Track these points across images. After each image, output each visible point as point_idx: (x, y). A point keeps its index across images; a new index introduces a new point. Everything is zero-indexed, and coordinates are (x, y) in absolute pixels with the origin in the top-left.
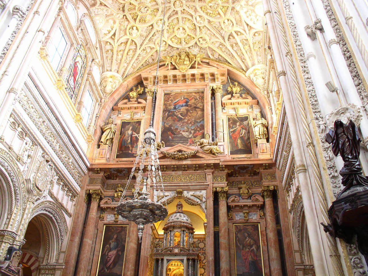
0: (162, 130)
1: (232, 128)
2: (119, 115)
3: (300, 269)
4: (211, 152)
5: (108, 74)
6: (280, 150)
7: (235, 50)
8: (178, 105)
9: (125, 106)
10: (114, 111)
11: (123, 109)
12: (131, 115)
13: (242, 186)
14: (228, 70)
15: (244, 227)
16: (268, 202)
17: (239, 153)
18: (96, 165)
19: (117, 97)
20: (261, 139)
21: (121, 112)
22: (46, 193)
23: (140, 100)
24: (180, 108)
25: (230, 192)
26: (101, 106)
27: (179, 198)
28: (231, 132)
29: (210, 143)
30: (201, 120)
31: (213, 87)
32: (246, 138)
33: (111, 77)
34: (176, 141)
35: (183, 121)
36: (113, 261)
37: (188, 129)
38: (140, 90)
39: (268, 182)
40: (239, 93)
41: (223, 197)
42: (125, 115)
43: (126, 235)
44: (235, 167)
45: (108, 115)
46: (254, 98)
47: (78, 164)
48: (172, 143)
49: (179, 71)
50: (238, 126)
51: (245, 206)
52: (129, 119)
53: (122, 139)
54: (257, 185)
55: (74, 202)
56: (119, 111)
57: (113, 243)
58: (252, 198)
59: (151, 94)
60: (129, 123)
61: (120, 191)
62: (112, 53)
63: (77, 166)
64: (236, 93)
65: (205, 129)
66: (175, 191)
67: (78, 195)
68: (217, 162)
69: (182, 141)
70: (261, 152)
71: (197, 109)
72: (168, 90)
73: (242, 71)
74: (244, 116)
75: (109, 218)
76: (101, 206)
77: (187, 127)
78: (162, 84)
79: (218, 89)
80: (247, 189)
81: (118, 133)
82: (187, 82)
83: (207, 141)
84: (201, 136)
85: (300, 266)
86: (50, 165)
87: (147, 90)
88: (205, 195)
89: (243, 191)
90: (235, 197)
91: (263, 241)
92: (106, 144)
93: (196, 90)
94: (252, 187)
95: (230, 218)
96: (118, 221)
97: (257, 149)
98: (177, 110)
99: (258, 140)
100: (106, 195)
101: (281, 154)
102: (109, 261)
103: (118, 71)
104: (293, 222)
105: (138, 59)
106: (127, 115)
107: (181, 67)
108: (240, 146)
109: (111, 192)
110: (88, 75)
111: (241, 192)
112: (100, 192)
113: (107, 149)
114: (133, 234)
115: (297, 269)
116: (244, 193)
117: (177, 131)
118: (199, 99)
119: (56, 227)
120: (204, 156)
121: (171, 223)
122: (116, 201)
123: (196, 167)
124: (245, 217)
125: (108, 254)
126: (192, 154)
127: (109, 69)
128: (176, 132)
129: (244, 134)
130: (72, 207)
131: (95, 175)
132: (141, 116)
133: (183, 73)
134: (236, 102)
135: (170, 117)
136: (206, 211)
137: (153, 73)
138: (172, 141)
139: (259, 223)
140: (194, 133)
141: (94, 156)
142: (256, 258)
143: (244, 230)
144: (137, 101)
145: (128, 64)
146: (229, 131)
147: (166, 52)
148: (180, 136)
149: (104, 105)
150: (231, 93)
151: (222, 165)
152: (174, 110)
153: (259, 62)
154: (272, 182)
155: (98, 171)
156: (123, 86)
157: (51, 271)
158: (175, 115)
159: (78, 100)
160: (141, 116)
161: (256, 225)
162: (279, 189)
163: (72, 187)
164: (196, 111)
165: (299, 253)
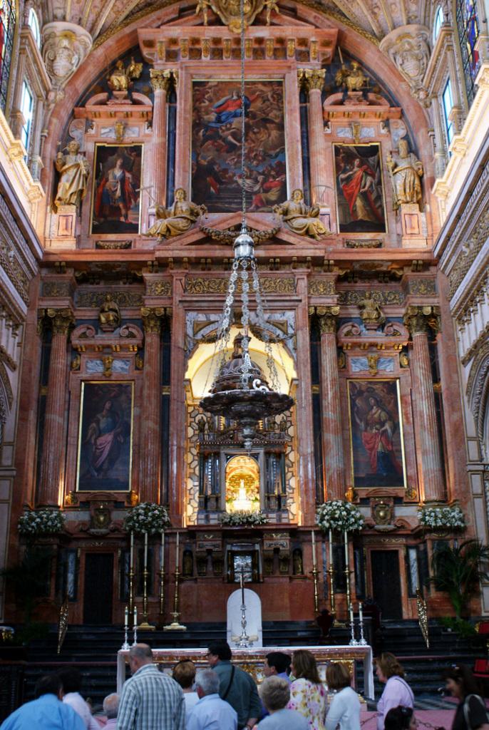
0: (194, 172)
1: (345, 171)
2: (90, 130)
3: (475, 472)
6: (454, 240)
8: (224, 113)
9: (103, 109)
10: (76, 121)
12: (117, 132)
13: (366, 302)
15: (369, 385)
16: (419, 336)
17: (358, 230)
19: (81, 85)
20: (407, 202)
21: (94, 123)
23: (136, 96)
24: (231, 120)
25: (344, 314)
26: (49, 110)
28: (342, 180)
29: (303, 212)
30: (278, 150)
32: (373, 196)
33: (66, 36)
34: (224, 198)
36: (108, 455)
37: (251, 171)
38: (136, 69)
39: (421, 297)
41: (329, 327)
42: (103, 131)
43: (131, 403)
44: (354, 264)
45: (64, 130)
47: (24, 258)
48: (216, 202)
49: (229, 29)
50: (359, 166)
52: (112, 140)
53: (100, 190)
54: (395, 301)
55: (17, 337)
56: (87, 119)
57: (105, 419)
58: (386, 328)
60: (113, 151)
63: (20, 260)
64: (354, 90)
67: (25, 323)
68: (319, 253)
70: (409, 232)
71: (268, 125)
74: (369, 145)
75: (92, 368)
77: (248, 168)
79: (315, 80)
80: (377, 309)
81: (93, 174)
83: (298, 206)
84: (279, 188)
85: (477, 466)
87: (152, 73)
88: (291, 322)
90: (353, 326)
91: (405, 414)
92: (69, 204)
94: (386, 304)
95: (343, 367)
97: (399, 224)
98: (224, 124)
99: (403, 206)
101: (456, 247)
102: (100, 456)
103: (80, 19)
104: (469, 385)
106: (107, 130)
108: (361, 215)
109: (89, 311)
110: (22, 38)
111: (365, 316)
112: (70, 314)
113: (75, 215)
114: (151, 404)
115: (470, 471)
116: (370, 319)
117: (227, 176)
118: (271, 100)
120: (291, 239)
121: (228, 379)
122: (105, 332)
123: (275, 263)
124: (371, 367)
125: (95, 442)
126: (267, 236)
127: (59, 13)
129: (369, 187)
130: (14, 350)
131: (54, 275)
132: (142, 134)
133: (237, 36)
134: (354, 112)
135: (210, 142)
136: (295, 355)
137: (167, 30)
138: (217, 198)
139: (399, 378)
140: (264, 181)
141: (47, 231)
142: (390, 447)
143: (368, 392)
144: (129, 97)
146: (337, 178)
148: (234, 188)
149: (55, 107)
153: (413, 18)
154: (428, 297)
155: (61, 267)
158: (220, 137)
159: (10, 106)
160: (142, 134)
161: (391, 383)
162: (442, 314)
163: (15, 309)
164: (267, 129)
165: (476, 442)
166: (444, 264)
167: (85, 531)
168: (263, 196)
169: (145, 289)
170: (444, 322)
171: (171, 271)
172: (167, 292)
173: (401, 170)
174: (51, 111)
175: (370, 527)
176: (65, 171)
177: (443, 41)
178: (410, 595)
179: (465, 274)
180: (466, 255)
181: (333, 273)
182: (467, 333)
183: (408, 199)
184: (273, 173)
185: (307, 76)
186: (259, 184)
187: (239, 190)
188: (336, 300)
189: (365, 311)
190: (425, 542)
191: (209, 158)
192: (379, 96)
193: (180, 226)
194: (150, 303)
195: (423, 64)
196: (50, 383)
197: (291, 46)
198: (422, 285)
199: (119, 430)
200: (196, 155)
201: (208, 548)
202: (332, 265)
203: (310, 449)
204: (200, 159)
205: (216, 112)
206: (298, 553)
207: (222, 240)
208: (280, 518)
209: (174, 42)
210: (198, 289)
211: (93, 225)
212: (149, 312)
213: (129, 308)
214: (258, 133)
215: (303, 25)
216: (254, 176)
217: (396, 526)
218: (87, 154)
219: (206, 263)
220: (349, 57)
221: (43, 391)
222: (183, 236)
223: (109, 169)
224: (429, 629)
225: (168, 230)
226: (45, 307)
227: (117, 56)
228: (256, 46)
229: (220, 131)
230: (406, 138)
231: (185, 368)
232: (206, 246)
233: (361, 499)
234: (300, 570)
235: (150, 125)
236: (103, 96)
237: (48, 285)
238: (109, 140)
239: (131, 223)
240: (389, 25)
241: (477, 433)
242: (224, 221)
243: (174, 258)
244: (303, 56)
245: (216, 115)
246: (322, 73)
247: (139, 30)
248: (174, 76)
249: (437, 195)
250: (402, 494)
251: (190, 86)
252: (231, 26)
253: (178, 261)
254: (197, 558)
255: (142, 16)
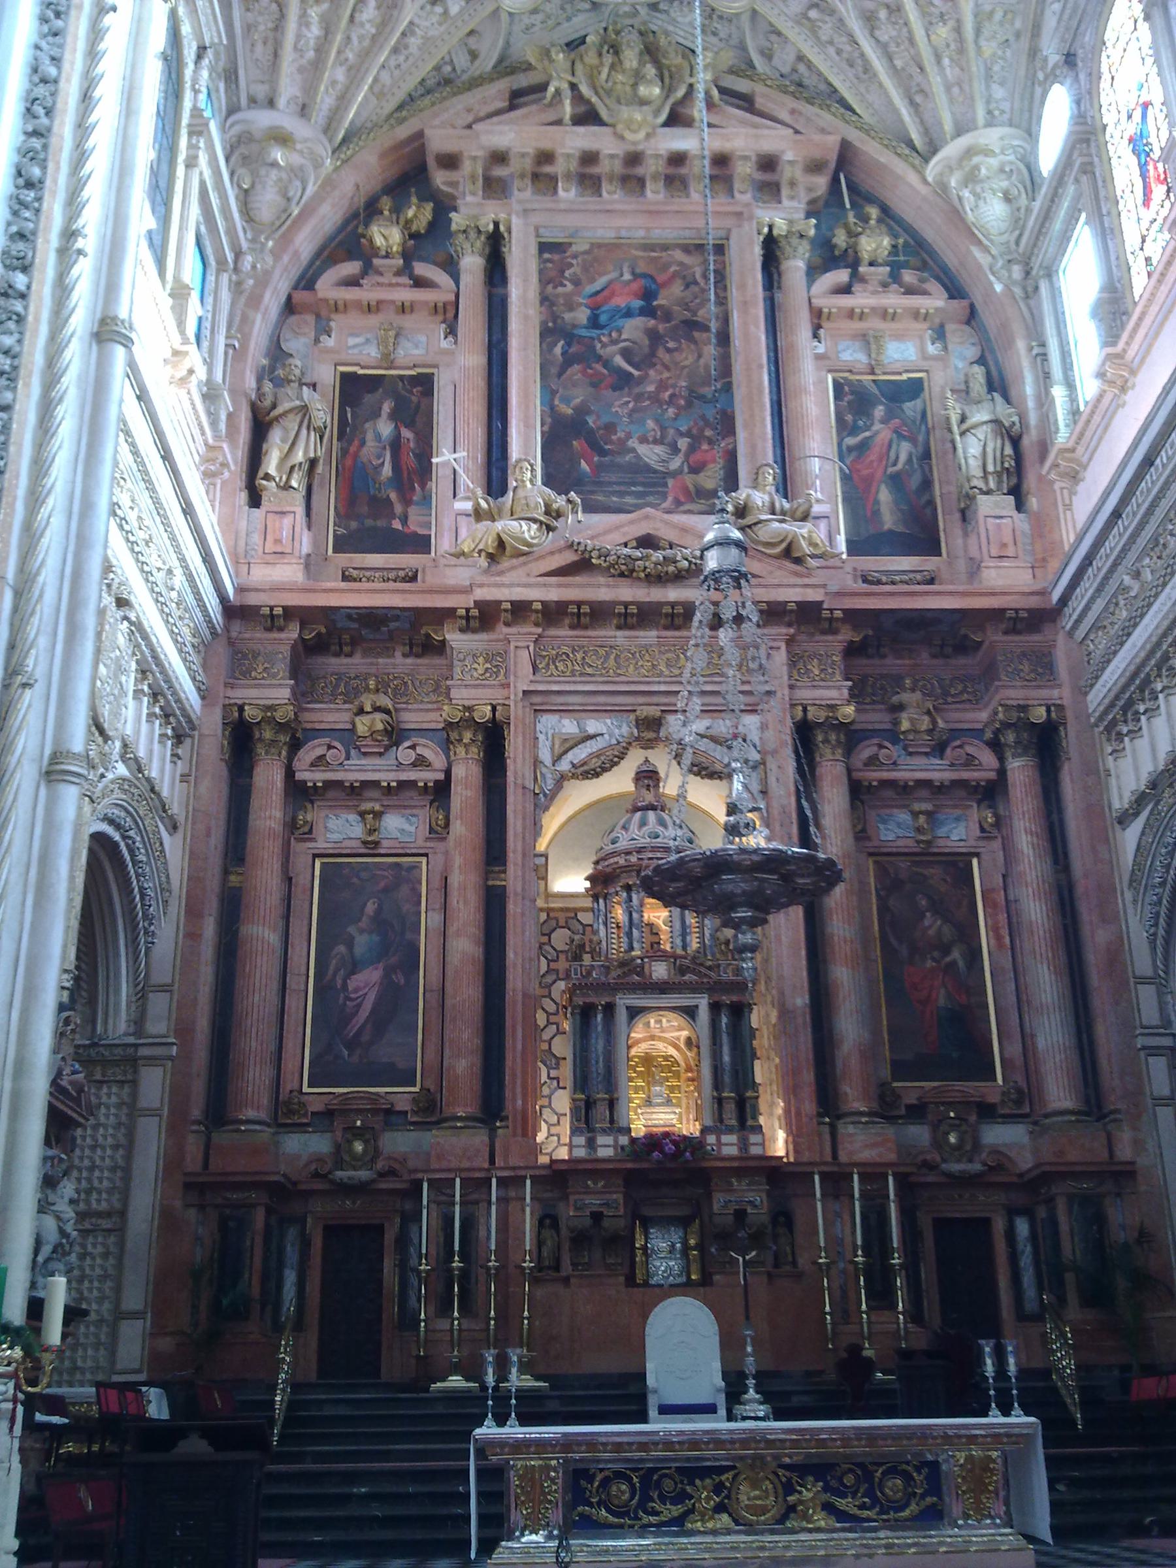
0: (546, 428)
1: (854, 431)
2: (323, 338)
4: (789, 553)
5: (263, 119)
6: (1102, 563)
7: (884, 38)
11: (341, 307)
14: (845, 148)
16: (1020, 770)
18: (263, 591)
19: (305, 243)
21: (333, 324)
22: (118, 744)
23: (422, 269)
24: (620, 322)
27: (648, 745)
28: (850, 449)
29: (777, 505)
31: (771, 227)
32: (915, 481)
34: (610, 484)
35: (637, 390)
36: (374, 1011)
37: (663, 429)
38: (419, 214)
39: (1022, 687)
40: (887, 264)
42: (352, 341)
46: (955, 291)
48: (593, 492)
49: (615, 134)
50: (882, 422)
51: (921, 783)
53: (349, 462)
54: (966, 696)
56: (318, 316)
58: (948, 751)
59: (478, 244)
60: (373, 383)
61: (377, 709)
62: (274, 6)
64: (871, 264)
65: (741, 435)
66: (632, 717)
69: (640, 489)
70: (994, 553)
71: (696, 334)
72: (557, 227)
73: (907, 151)
74: (905, 377)
76: (299, 776)
77: (657, 421)
78: (528, 194)
79: (795, 241)
80: (929, 713)
82: (649, 193)
83: (766, 498)
86: (126, 618)
87: (457, 220)
89: (912, 724)
90: (881, 746)
91: (994, 929)
93: (687, 233)
96: (377, 844)
99: (981, 499)
100: (309, 726)
103: (304, 107)
105: (406, 47)
107: (625, 112)
108: (889, 520)
110: (191, 134)
111: (905, 725)
115: (1144, 1048)
116: (916, 731)
119: (128, 881)
122: (365, 754)
127: (261, 91)
128: (611, 442)
131: (258, 635)
133: (631, 148)
134: (873, 309)
135: (576, 367)
139: (977, 855)
140: (692, 449)
145: (355, 73)
146: (840, 445)
147: (539, 17)
150: (849, 259)
151: (831, 610)
152: (594, 333)
153: (996, 113)
154: (1039, 687)
156: (337, 193)
157: (117, 1070)
158: (599, 358)
159: (169, 276)
163: (178, 701)
164: (696, 342)
166: (1075, 617)
167: (324, 1176)
168: (689, 480)
169: (451, 666)
170: (1071, 739)
171: (506, 630)
172: (497, 674)
173: (975, 426)
174: (246, 294)
175: (930, 1166)
176: (277, 419)
177: (1070, 156)
178: (1022, 1316)
179: (1129, 635)
180: (1133, 594)
181: (840, 637)
182: (1129, 759)
183: (992, 485)
184: (708, 433)
185: (775, 232)
186: (681, 455)
187: (640, 469)
188: (846, 692)
189: (904, 715)
190: (1050, 1201)
191: (578, 400)
192: (925, 274)
193: (526, 535)
194: (461, 696)
195: (1018, 210)
196: (248, 859)
197: (744, 170)
198: (1025, 662)
199: (393, 960)
200: (549, 393)
201: (595, 1209)
202: (837, 619)
203: (801, 1000)
204: (556, 402)
205: (587, 307)
206: (783, 1218)
207: (612, 565)
208: (744, 1145)
209: (499, 157)
210: (561, 666)
211: (335, 536)
212: (460, 714)
213: (415, 706)
214: (676, 349)
215: (769, 128)
216: (669, 439)
217: (985, 1164)
218: (318, 387)
219: (579, 615)
220: (861, 197)
221: (234, 879)
222: (530, 558)
223: (367, 421)
224: (1083, 1390)
225: (501, 544)
226: (239, 702)
227: (379, 187)
228: (671, 171)
229: (599, 346)
230: (981, 361)
231: (536, 829)
232: (578, 579)
233: (909, 1107)
234: (790, 1259)
235: (452, 331)
236: (351, 268)
237: (245, 656)
238: (364, 360)
239: (415, 534)
240: (948, 127)
241: (1155, 966)
242: (618, 528)
243: (512, 603)
244: (770, 190)
245: (588, 311)
246: (810, 227)
247: (427, 132)
248: (502, 228)
249: (1053, 476)
250: (994, 1098)
251: (533, 249)
252: (620, 127)
253: (520, 610)
254: (572, 1230)
255: (433, 104)
